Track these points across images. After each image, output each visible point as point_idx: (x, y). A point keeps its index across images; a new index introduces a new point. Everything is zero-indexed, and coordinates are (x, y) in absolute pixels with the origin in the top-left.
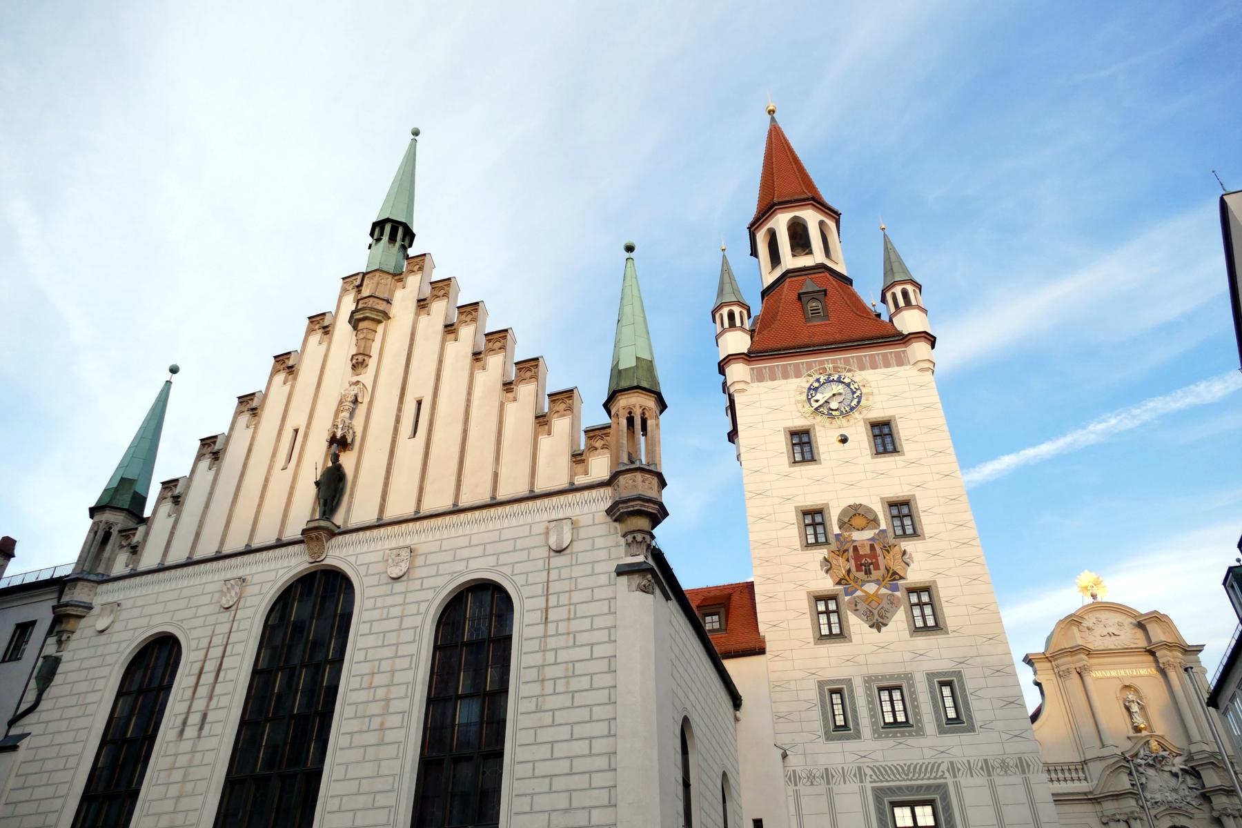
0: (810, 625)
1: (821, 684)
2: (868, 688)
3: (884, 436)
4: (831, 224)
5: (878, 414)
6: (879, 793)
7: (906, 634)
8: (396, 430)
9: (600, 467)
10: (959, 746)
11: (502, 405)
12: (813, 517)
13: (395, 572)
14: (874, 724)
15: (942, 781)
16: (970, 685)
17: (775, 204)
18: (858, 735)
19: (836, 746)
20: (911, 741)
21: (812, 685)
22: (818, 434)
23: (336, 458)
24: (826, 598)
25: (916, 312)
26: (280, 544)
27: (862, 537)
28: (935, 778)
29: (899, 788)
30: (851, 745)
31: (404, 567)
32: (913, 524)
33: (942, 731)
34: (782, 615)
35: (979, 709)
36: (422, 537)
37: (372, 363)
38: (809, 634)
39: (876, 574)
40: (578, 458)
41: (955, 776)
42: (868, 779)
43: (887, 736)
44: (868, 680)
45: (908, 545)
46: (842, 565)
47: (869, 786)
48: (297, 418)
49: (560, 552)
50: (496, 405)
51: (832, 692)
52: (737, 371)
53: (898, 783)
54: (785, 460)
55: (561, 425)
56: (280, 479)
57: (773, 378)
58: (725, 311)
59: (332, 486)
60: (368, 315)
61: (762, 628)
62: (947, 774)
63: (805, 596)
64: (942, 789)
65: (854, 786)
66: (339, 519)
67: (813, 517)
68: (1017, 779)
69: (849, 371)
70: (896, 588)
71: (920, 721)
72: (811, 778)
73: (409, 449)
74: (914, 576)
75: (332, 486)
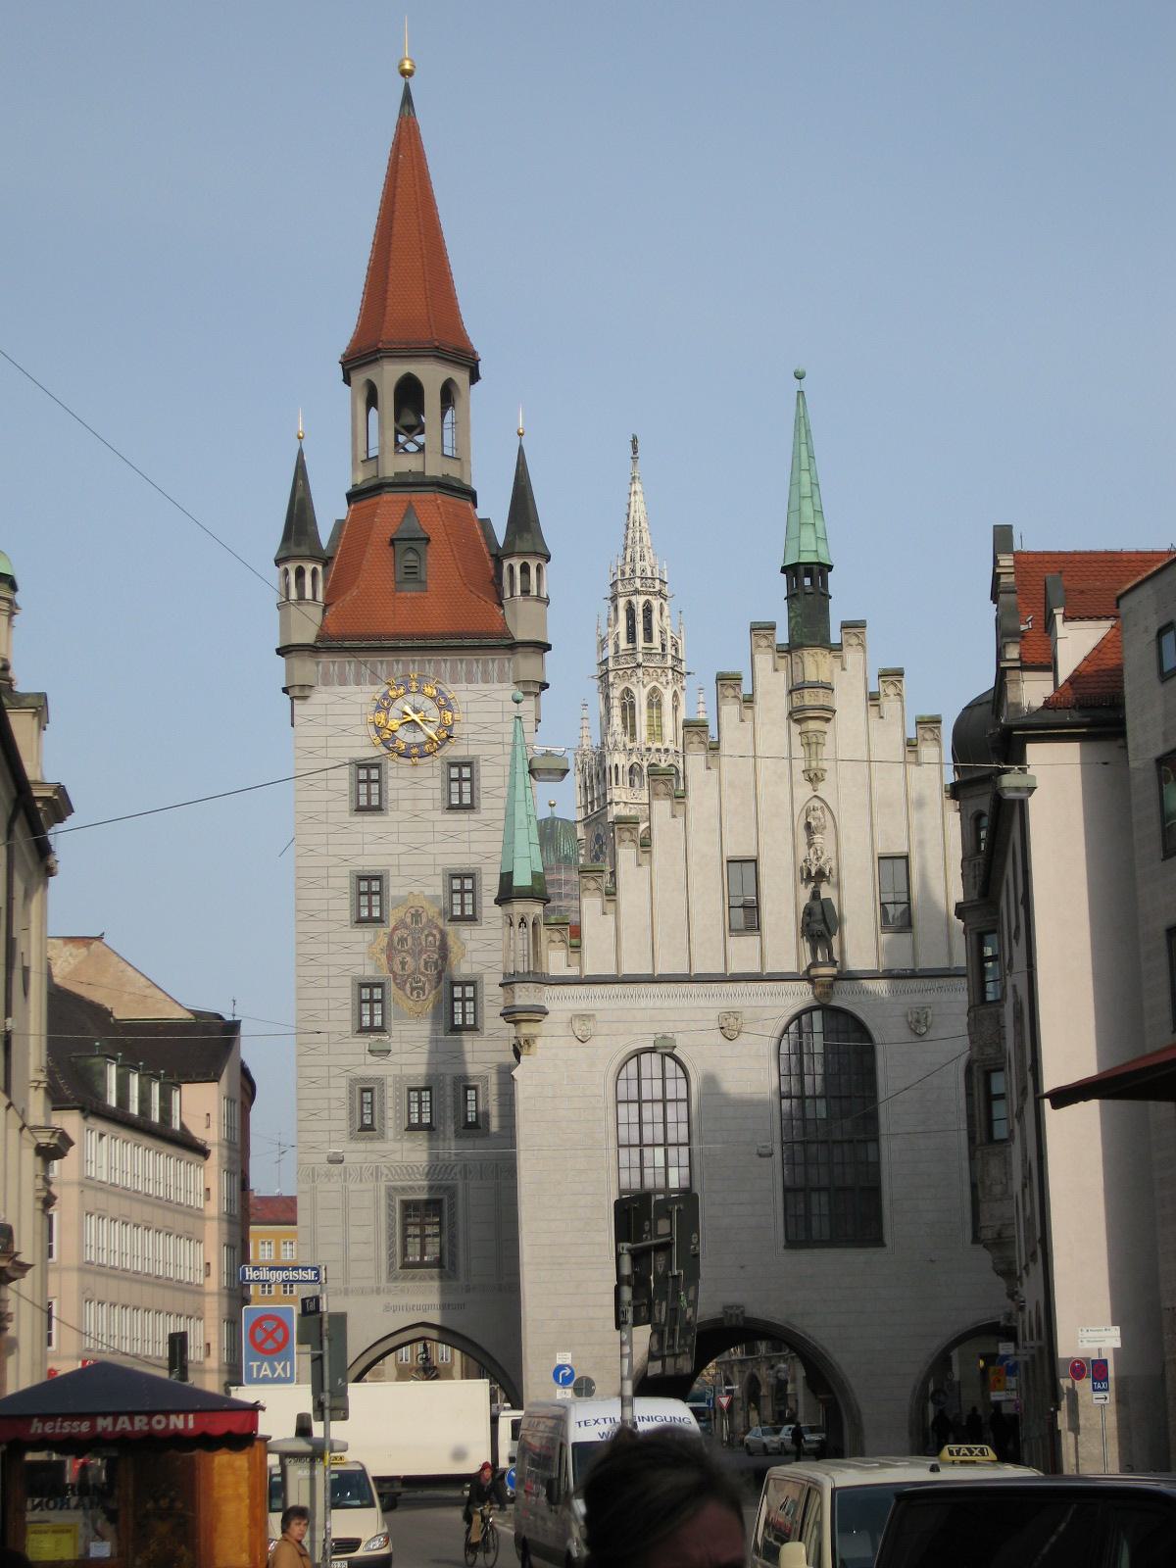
1: (354, 1081)
4: (461, 377)
6: (391, 1191)
15: (455, 1182)
17: (379, 350)
18: (382, 1137)
21: (344, 1083)
22: (391, 773)
24: (371, 986)
25: (533, 605)
28: (447, 1179)
29: (411, 1188)
32: (474, 904)
38: (348, 1027)
41: (466, 1178)
42: (384, 1176)
47: (383, 1186)
51: (364, 1090)
53: (410, 1183)
54: (345, 805)
57: (343, 682)
58: (292, 567)
62: (458, 1176)
63: (348, 982)
67: (370, 885)
69: (438, 682)
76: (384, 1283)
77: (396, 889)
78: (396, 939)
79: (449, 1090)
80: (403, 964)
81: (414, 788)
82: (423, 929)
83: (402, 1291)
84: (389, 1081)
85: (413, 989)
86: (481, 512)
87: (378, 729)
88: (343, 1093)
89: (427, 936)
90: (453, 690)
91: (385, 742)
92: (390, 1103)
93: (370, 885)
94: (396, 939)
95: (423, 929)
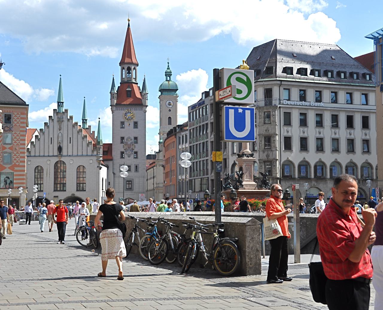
1: (120, 165)
3: (136, 124)
5: (135, 120)
7: (133, 158)
8: (68, 142)
9: (95, 153)
10: (136, 174)
11: (82, 142)
12: (122, 138)
13: (71, 163)
16: (139, 166)
23: (60, 145)
26: (53, 156)
27: (129, 143)
31: (72, 163)
33: (134, 172)
34: (116, 153)
35: (140, 169)
36: (74, 159)
37: (62, 129)
39: (130, 149)
40: (93, 151)
45: (136, 145)
46: (126, 147)
48: (51, 136)
49: (91, 163)
50: (81, 141)
52: (114, 108)
55: (90, 146)
56: (51, 146)
59: (60, 149)
60: (60, 121)
61: (113, 156)
66: (61, 154)
67: (122, 138)
68: (143, 178)
70: (132, 151)
73: (70, 145)
74: (135, 150)
75: (60, 149)
81: (128, 125)
86: (138, 85)
90: (135, 112)
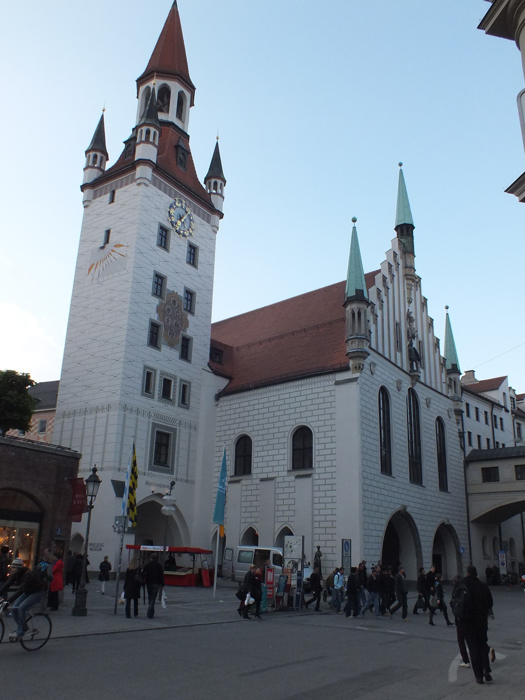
0: (147, 336)
2: (161, 377)
6: (154, 425)
12: (159, 280)
14: (159, 394)
18: (153, 397)
19: (144, 399)
20: (169, 406)
21: (142, 367)
29: (161, 425)
30: (150, 401)
42: (152, 418)
43: (162, 402)
44: (162, 373)
47: (151, 421)
57: (160, 189)
64: (174, 430)
65: (146, 419)
71: (174, 399)
72: (131, 410)
76: (147, 471)
77: (170, 286)
78: (166, 308)
79: (178, 384)
80: (168, 320)
82: (176, 308)
83: (153, 475)
84: (158, 372)
85: (170, 334)
87: (170, 215)
88: (141, 371)
89: (177, 312)
91: (172, 223)
92: (157, 382)
93: (159, 280)
94: (166, 308)
95: (176, 308)
